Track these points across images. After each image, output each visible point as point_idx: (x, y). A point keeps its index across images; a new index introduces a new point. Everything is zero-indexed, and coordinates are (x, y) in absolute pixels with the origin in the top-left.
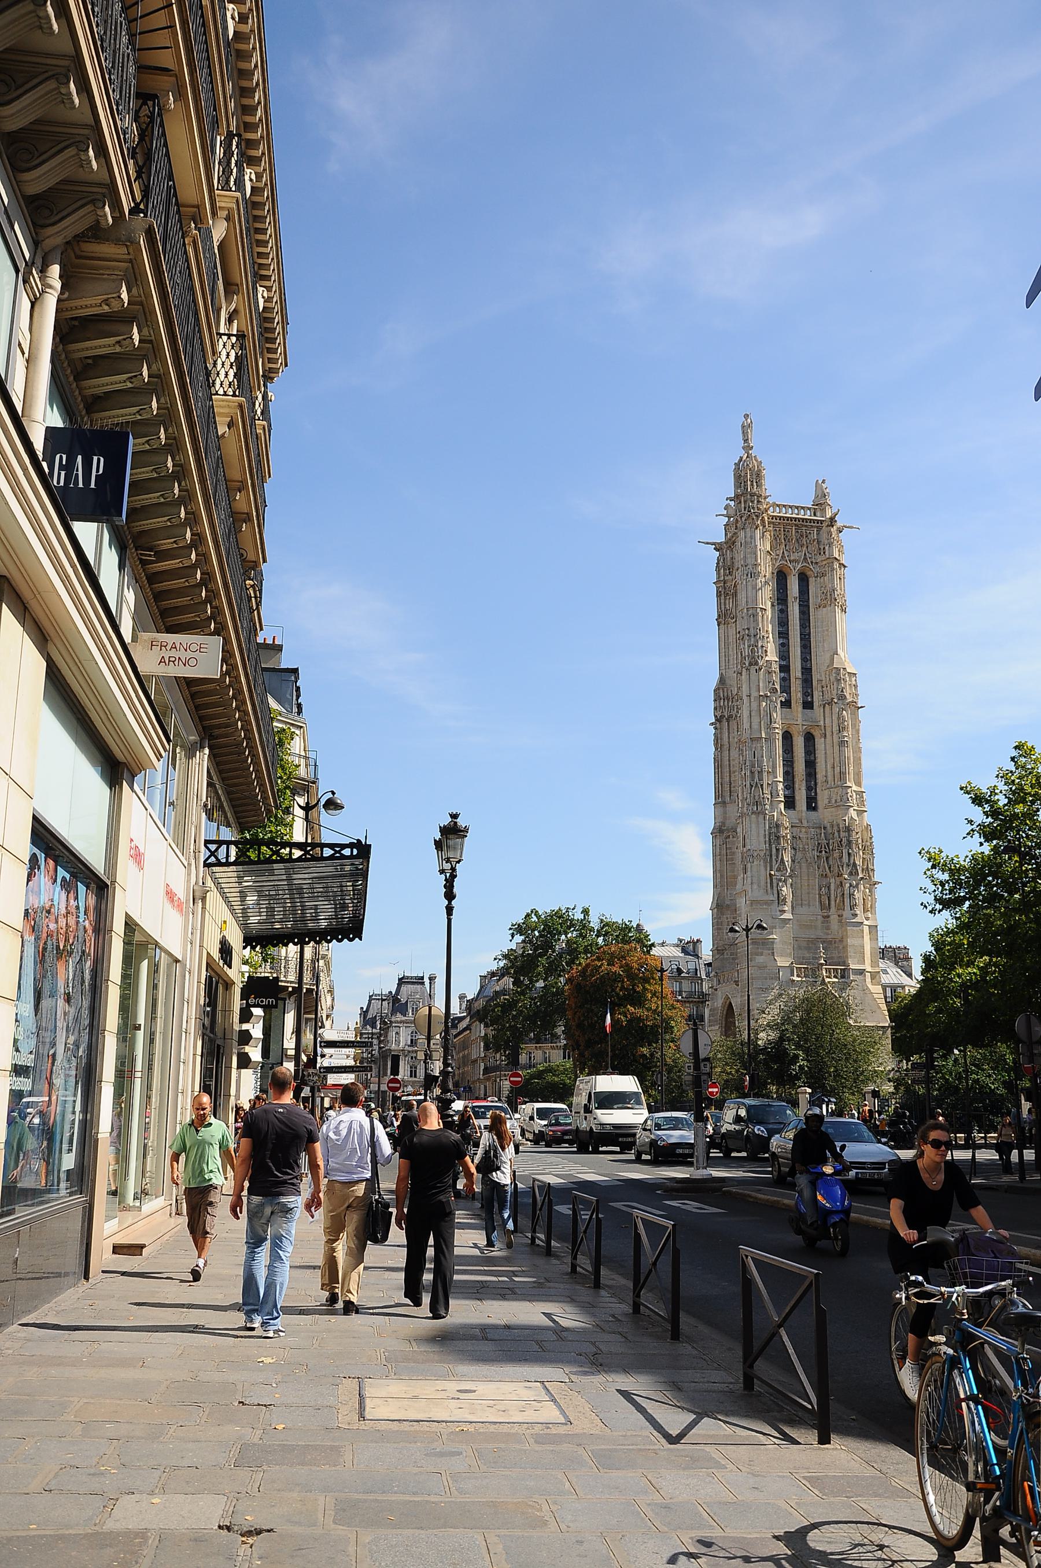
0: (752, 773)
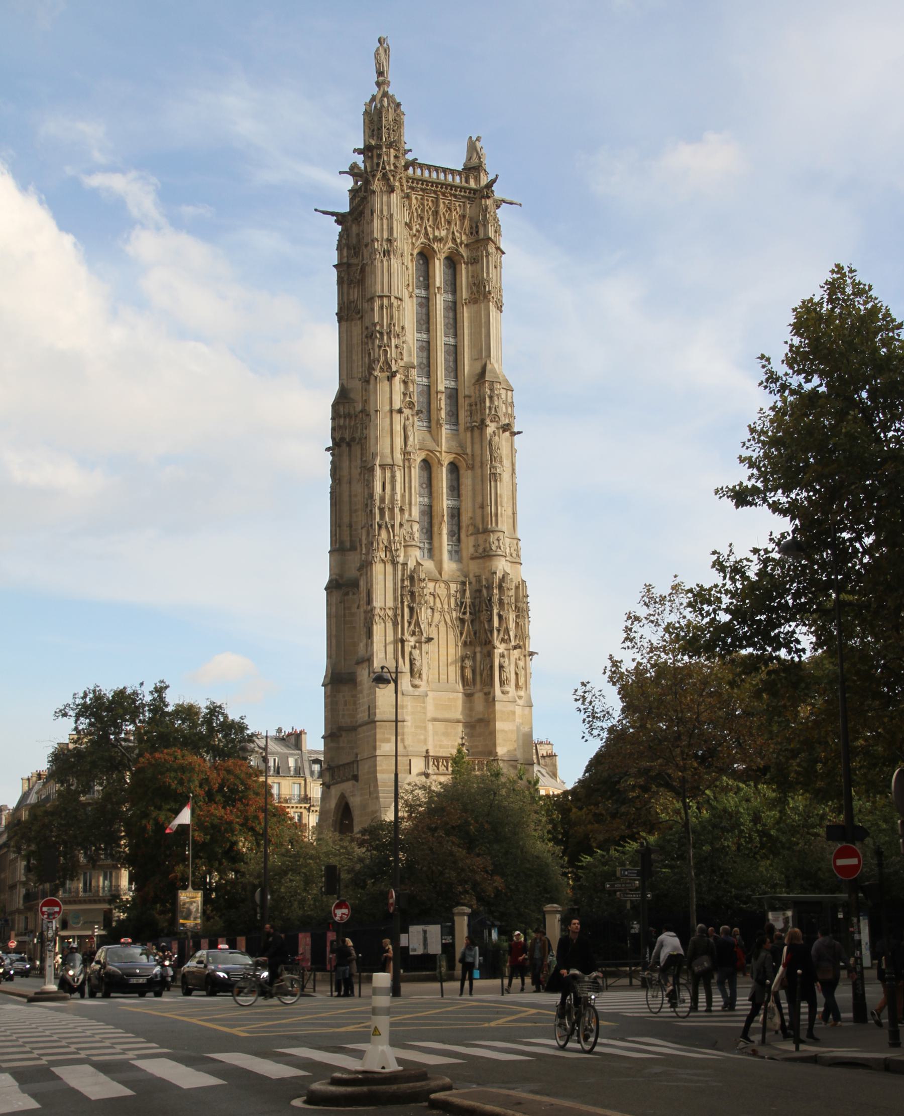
0: (382, 511)
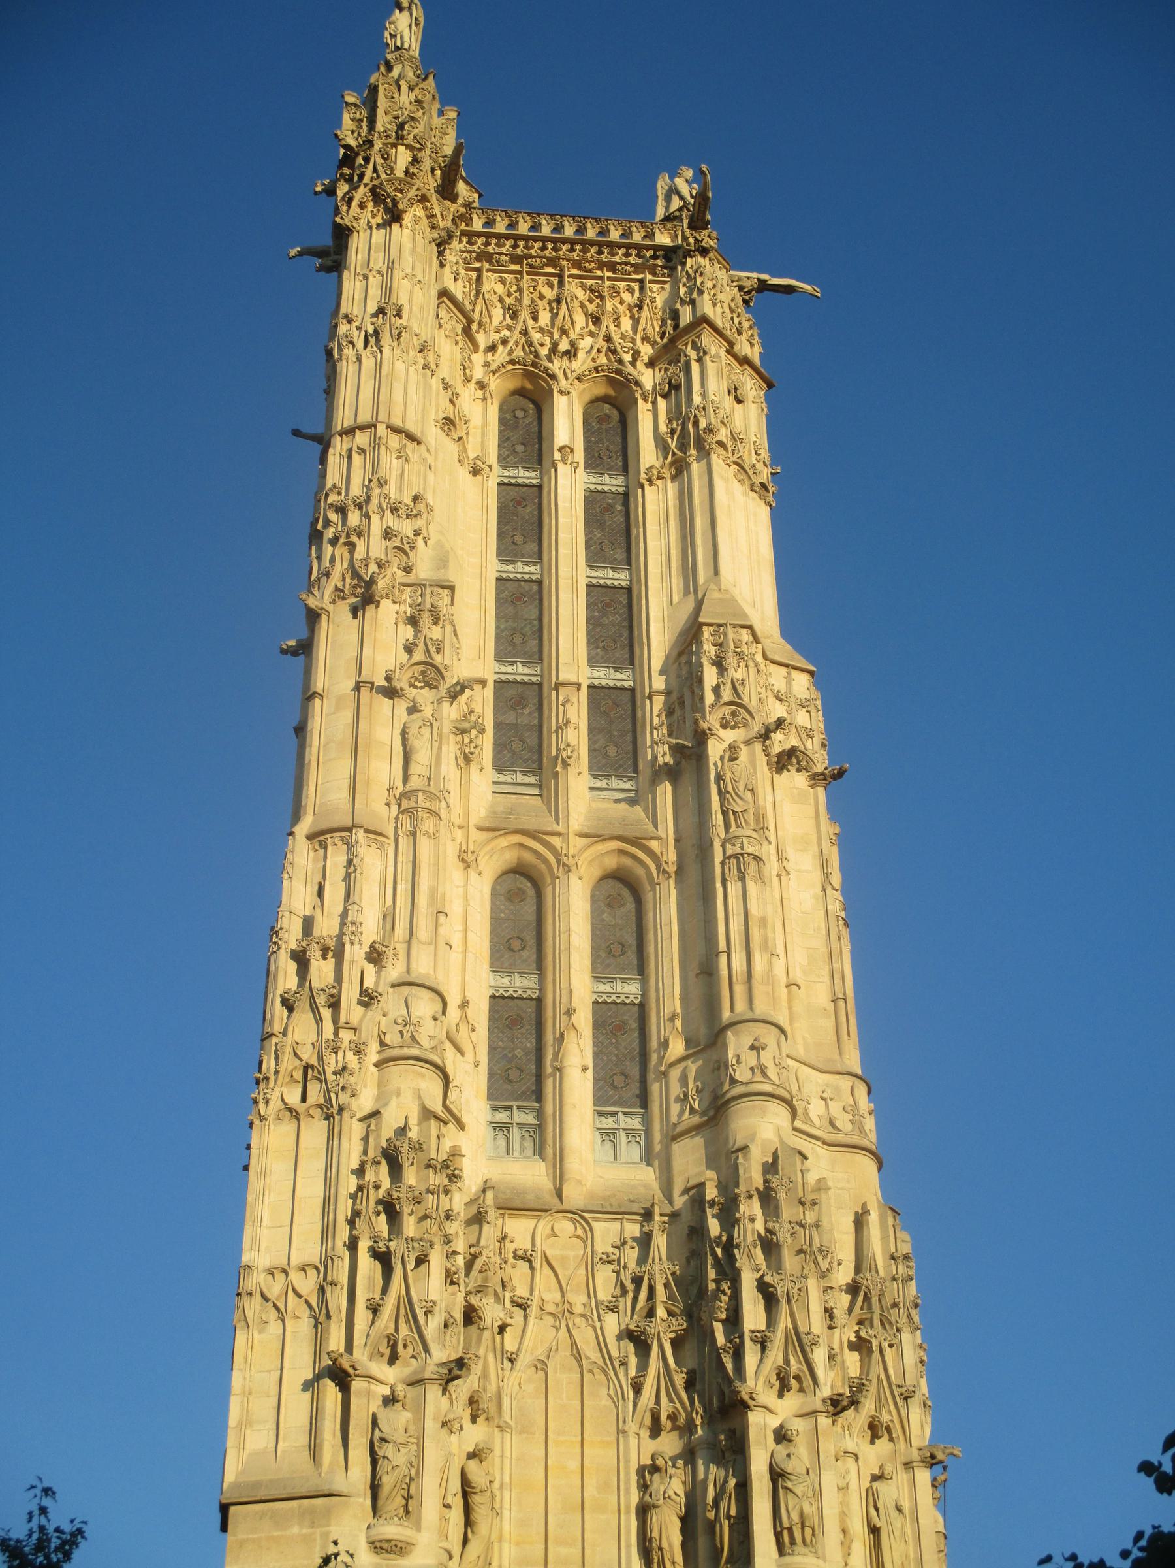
0: (301, 959)
